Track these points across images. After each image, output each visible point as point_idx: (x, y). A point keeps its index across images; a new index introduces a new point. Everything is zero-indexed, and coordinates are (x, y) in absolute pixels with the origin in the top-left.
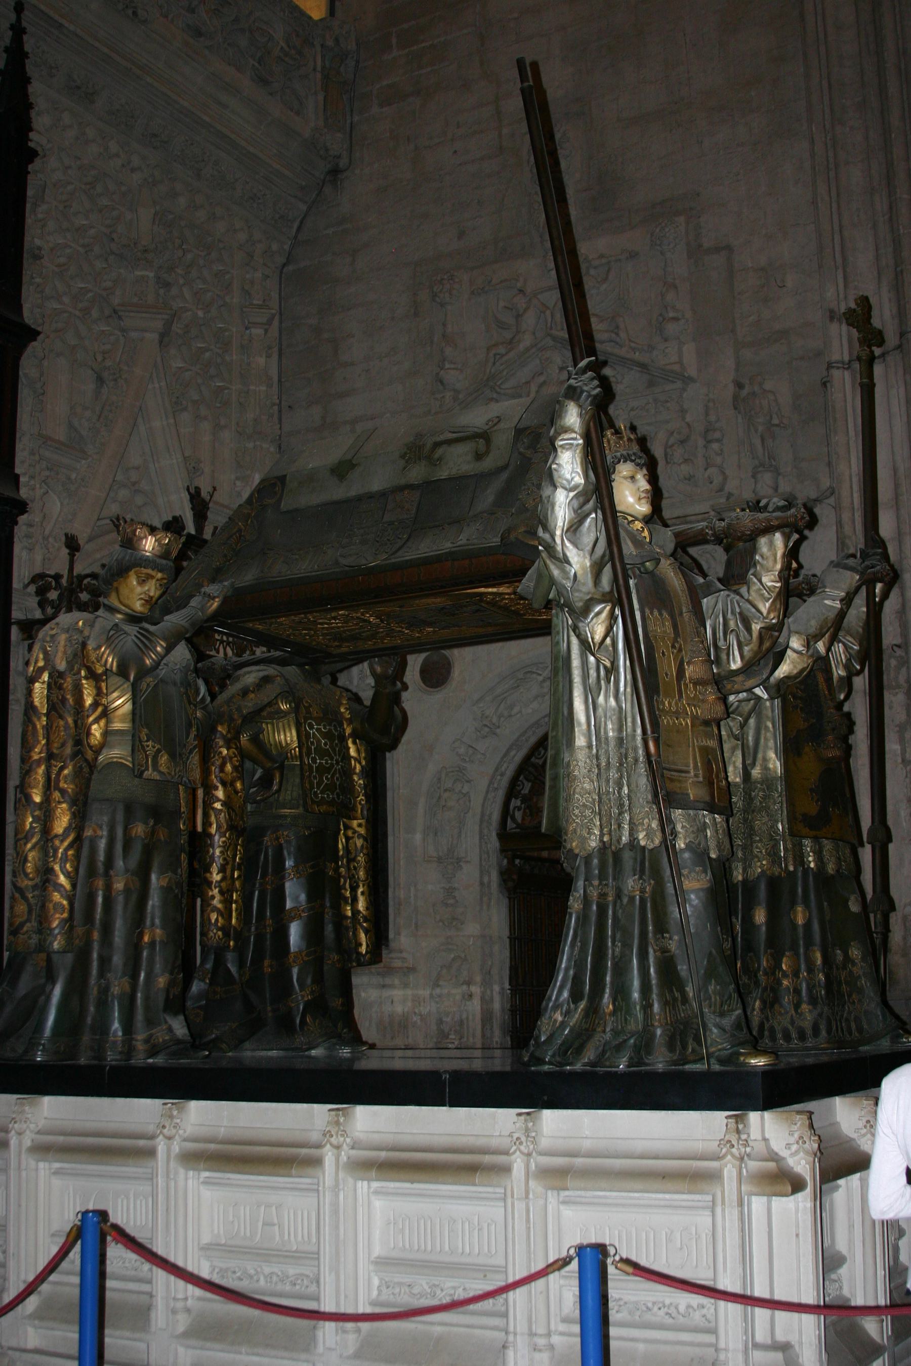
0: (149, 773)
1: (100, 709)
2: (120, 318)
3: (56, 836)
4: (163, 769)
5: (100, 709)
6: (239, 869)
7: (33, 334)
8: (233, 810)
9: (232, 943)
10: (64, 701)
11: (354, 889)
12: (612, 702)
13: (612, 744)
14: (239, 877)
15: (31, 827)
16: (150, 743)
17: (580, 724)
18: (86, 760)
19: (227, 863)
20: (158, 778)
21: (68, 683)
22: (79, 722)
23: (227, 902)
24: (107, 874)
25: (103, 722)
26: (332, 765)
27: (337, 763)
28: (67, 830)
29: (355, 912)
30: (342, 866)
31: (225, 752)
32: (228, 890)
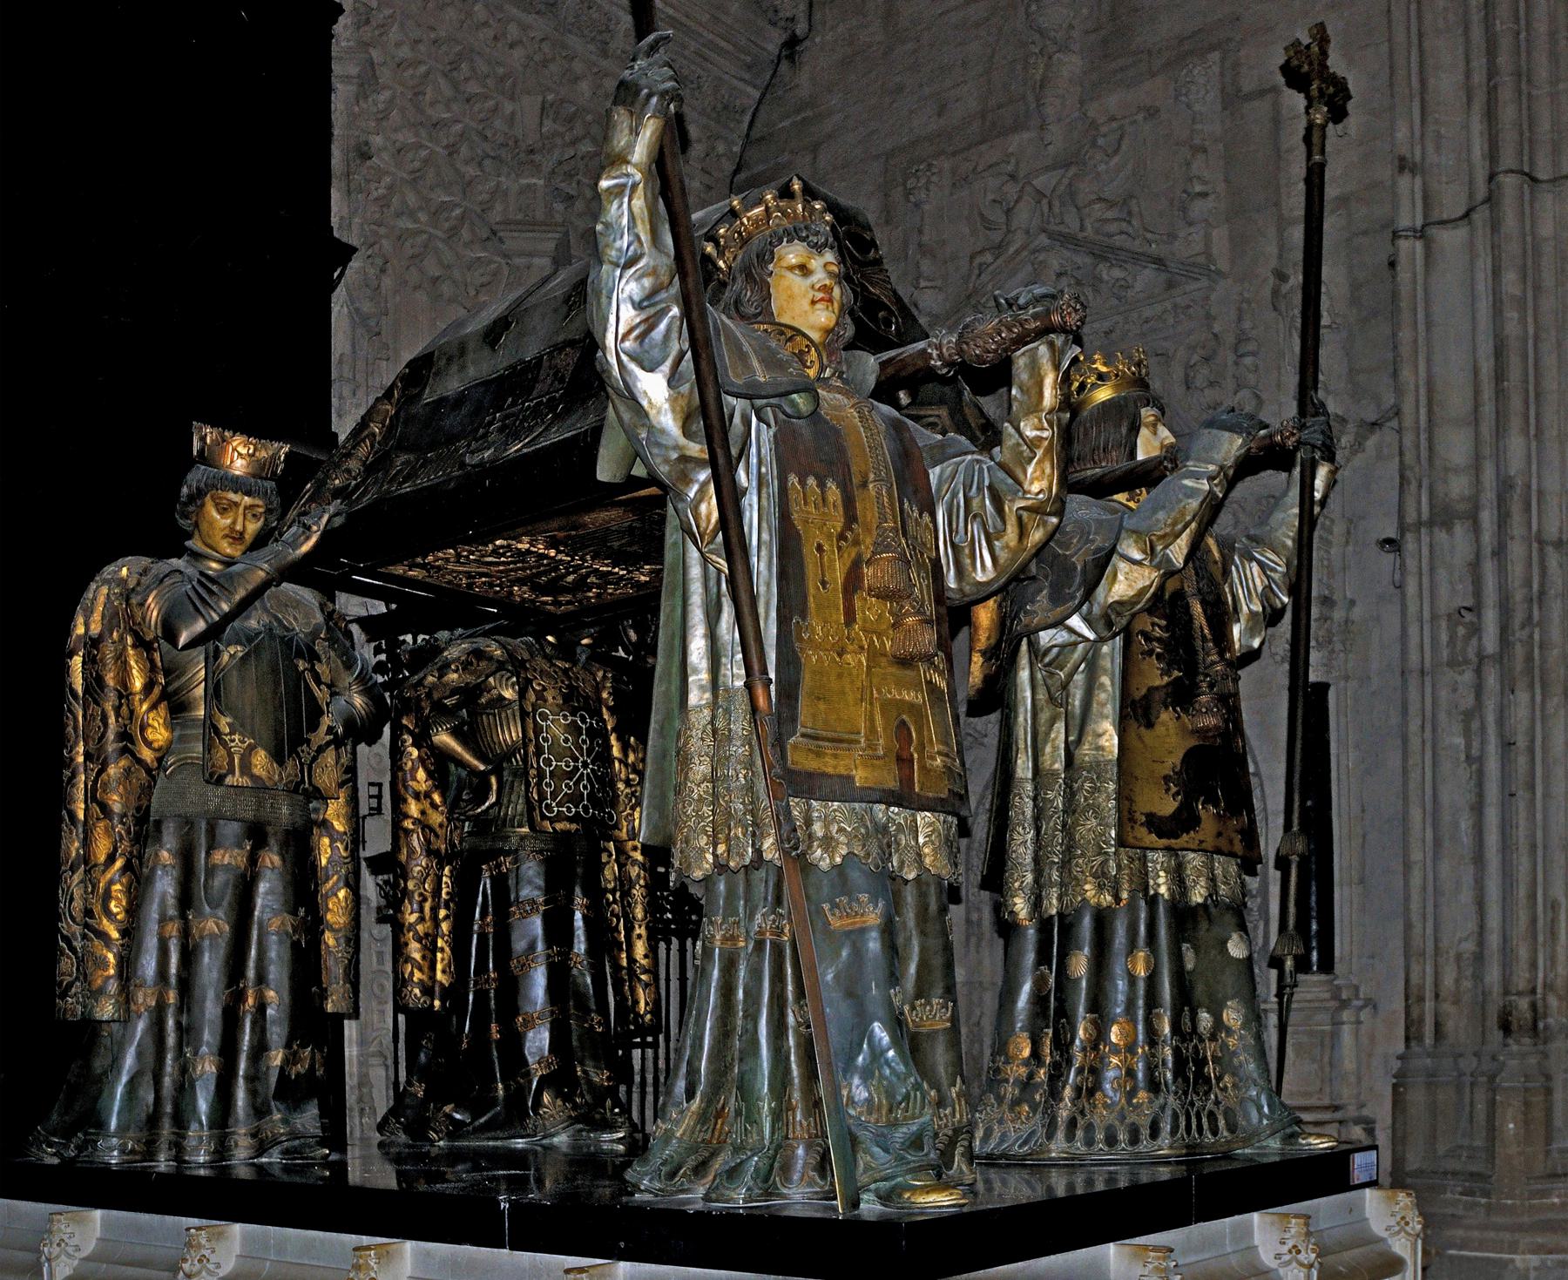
0: (236, 779)
4: (257, 771)
6: (447, 907)
9: (437, 1003)
11: (629, 929)
14: (447, 917)
16: (236, 737)
19: (425, 900)
21: (108, 651)
23: (431, 950)
24: (183, 916)
26: (576, 769)
27: (585, 765)
28: (111, 859)
29: (632, 960)
30: (615, 901)
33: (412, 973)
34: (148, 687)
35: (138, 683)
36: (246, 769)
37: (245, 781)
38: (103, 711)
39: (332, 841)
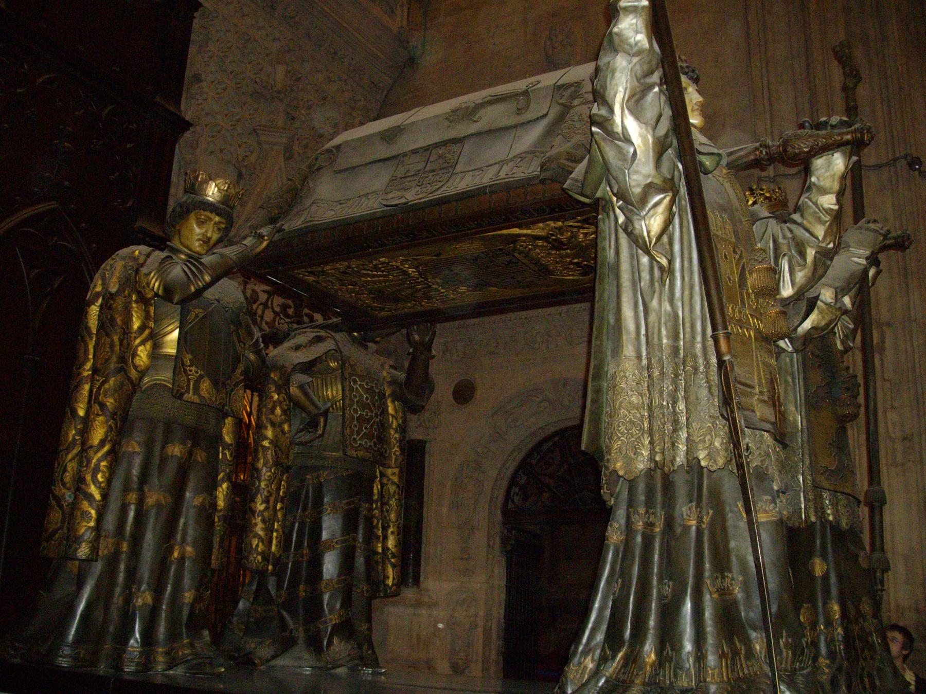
0: (190, 396)
1: (147, 332)
2: (257, 134)
3: (91, 447)
4: (204, 393)
5: (147, 332)
6: (282, 502)
7: (186, 125)
8: (280, 449)
9: (270, 567)
10: (112, 320)
11: (385, 529)
12: (667, 306)
13: (667, 352)
14: (282, 508)
15: (74, 439)
16: (193, 368)
17: (628, 333)
18: (129, 379)
19: (271, 495)
20: (198, 401)
22: (125, 341)
23: (269, 530)
24: (141, 489)
25: (149, 345)
26: (372, 417)
27: (377, 415)
28: (102, 443)
29: (385, 549)
30: (376, 508)
31: (276, 397)
32: (270, 520)
33: (257, 545)
34: (142, 328)
35: (136, 324)
36: (197, 390)
37: (195, 399)
38: (112, 340)
39: (224, 449)
